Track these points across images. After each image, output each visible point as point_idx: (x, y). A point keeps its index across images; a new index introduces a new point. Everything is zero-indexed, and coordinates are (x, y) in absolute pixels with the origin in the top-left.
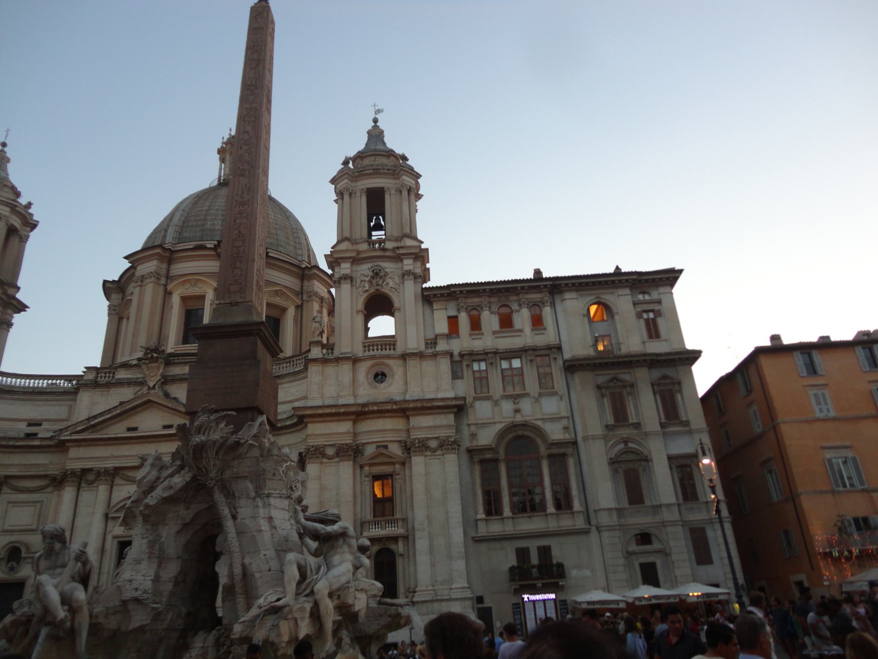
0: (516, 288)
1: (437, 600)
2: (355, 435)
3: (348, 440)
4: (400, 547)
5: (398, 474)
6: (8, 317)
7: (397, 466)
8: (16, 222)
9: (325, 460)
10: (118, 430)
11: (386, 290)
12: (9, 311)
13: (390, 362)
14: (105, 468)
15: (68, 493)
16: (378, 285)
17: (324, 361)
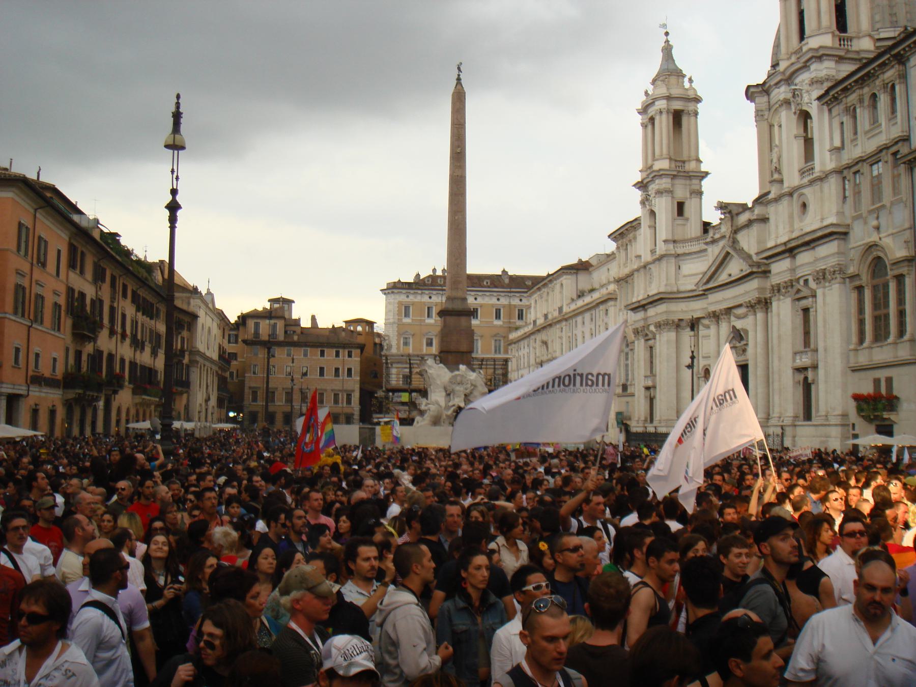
0: (869, 72)
1: (825, 425)
2: (793, 270)
3: (787, 277)
4: (810, 375)
5: (812, 307)
6: (696, 187)
7: (810, 299)
8: (677, 105)
9: (782, 297)
10: (723, 278)
11: (805, 108)
12: (695, 181)
13: (805, 191)
14: (721, 310)
15: (713, 328)
16: (798, 104)
17: (777, 200)
